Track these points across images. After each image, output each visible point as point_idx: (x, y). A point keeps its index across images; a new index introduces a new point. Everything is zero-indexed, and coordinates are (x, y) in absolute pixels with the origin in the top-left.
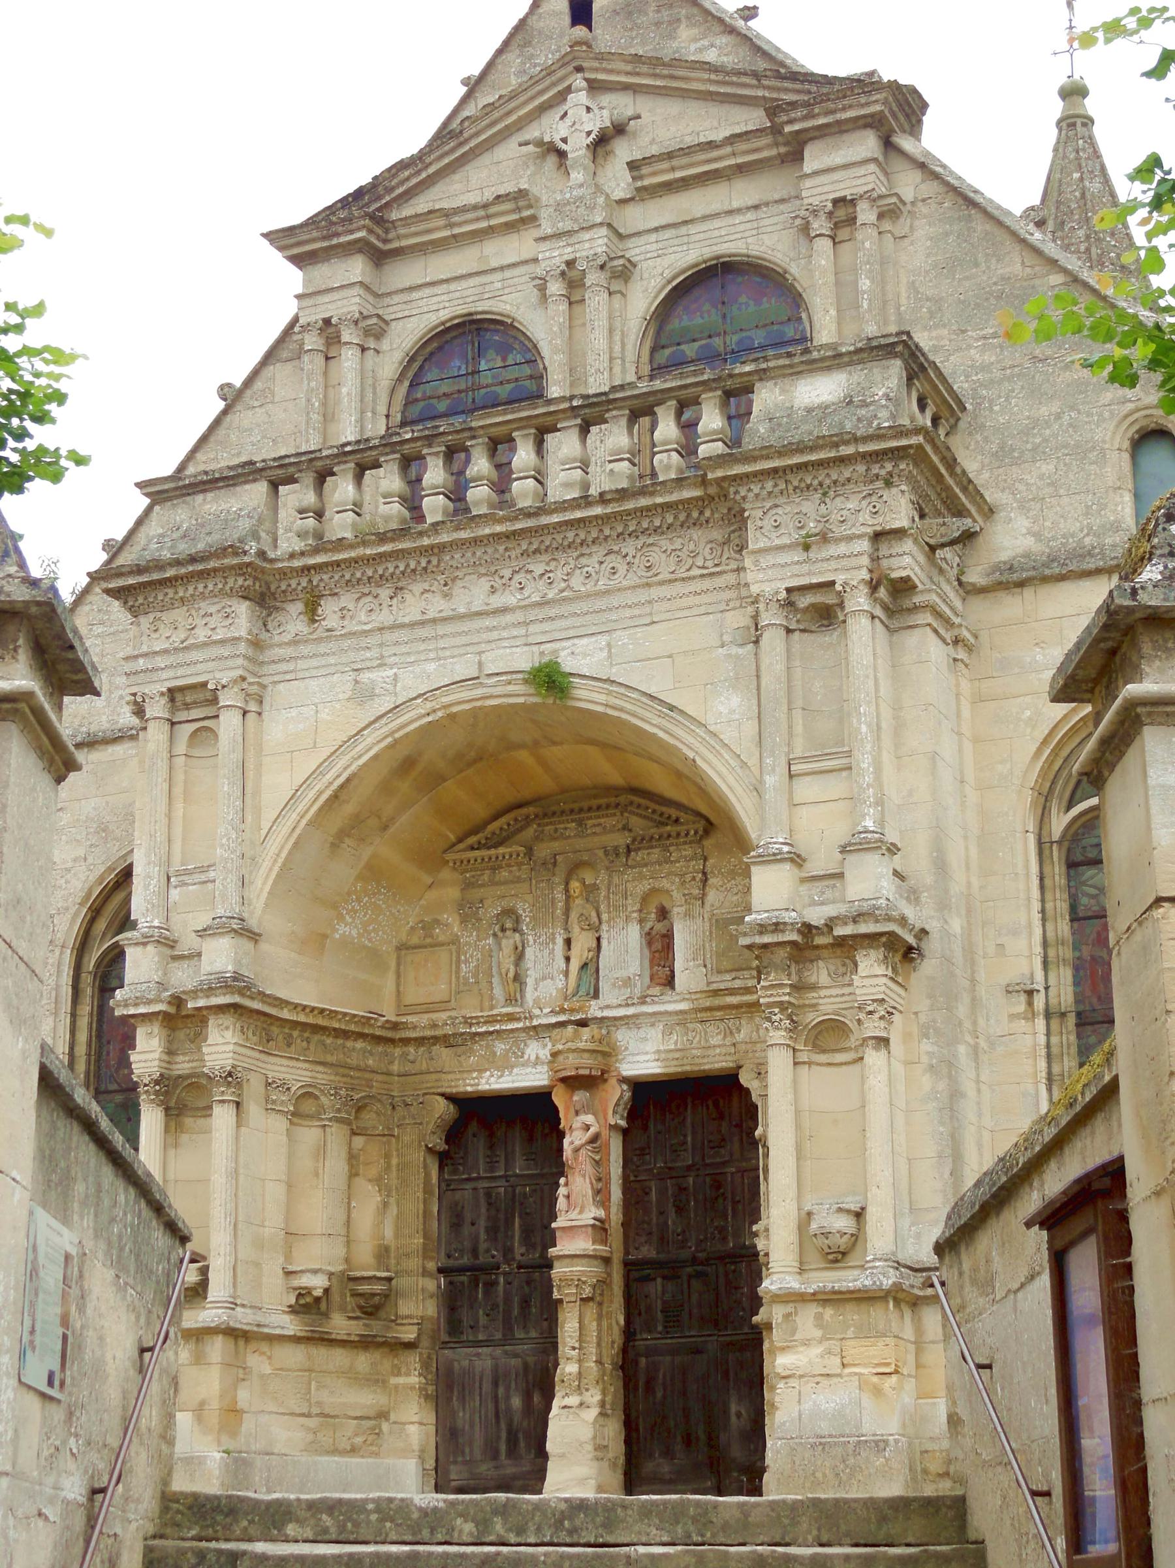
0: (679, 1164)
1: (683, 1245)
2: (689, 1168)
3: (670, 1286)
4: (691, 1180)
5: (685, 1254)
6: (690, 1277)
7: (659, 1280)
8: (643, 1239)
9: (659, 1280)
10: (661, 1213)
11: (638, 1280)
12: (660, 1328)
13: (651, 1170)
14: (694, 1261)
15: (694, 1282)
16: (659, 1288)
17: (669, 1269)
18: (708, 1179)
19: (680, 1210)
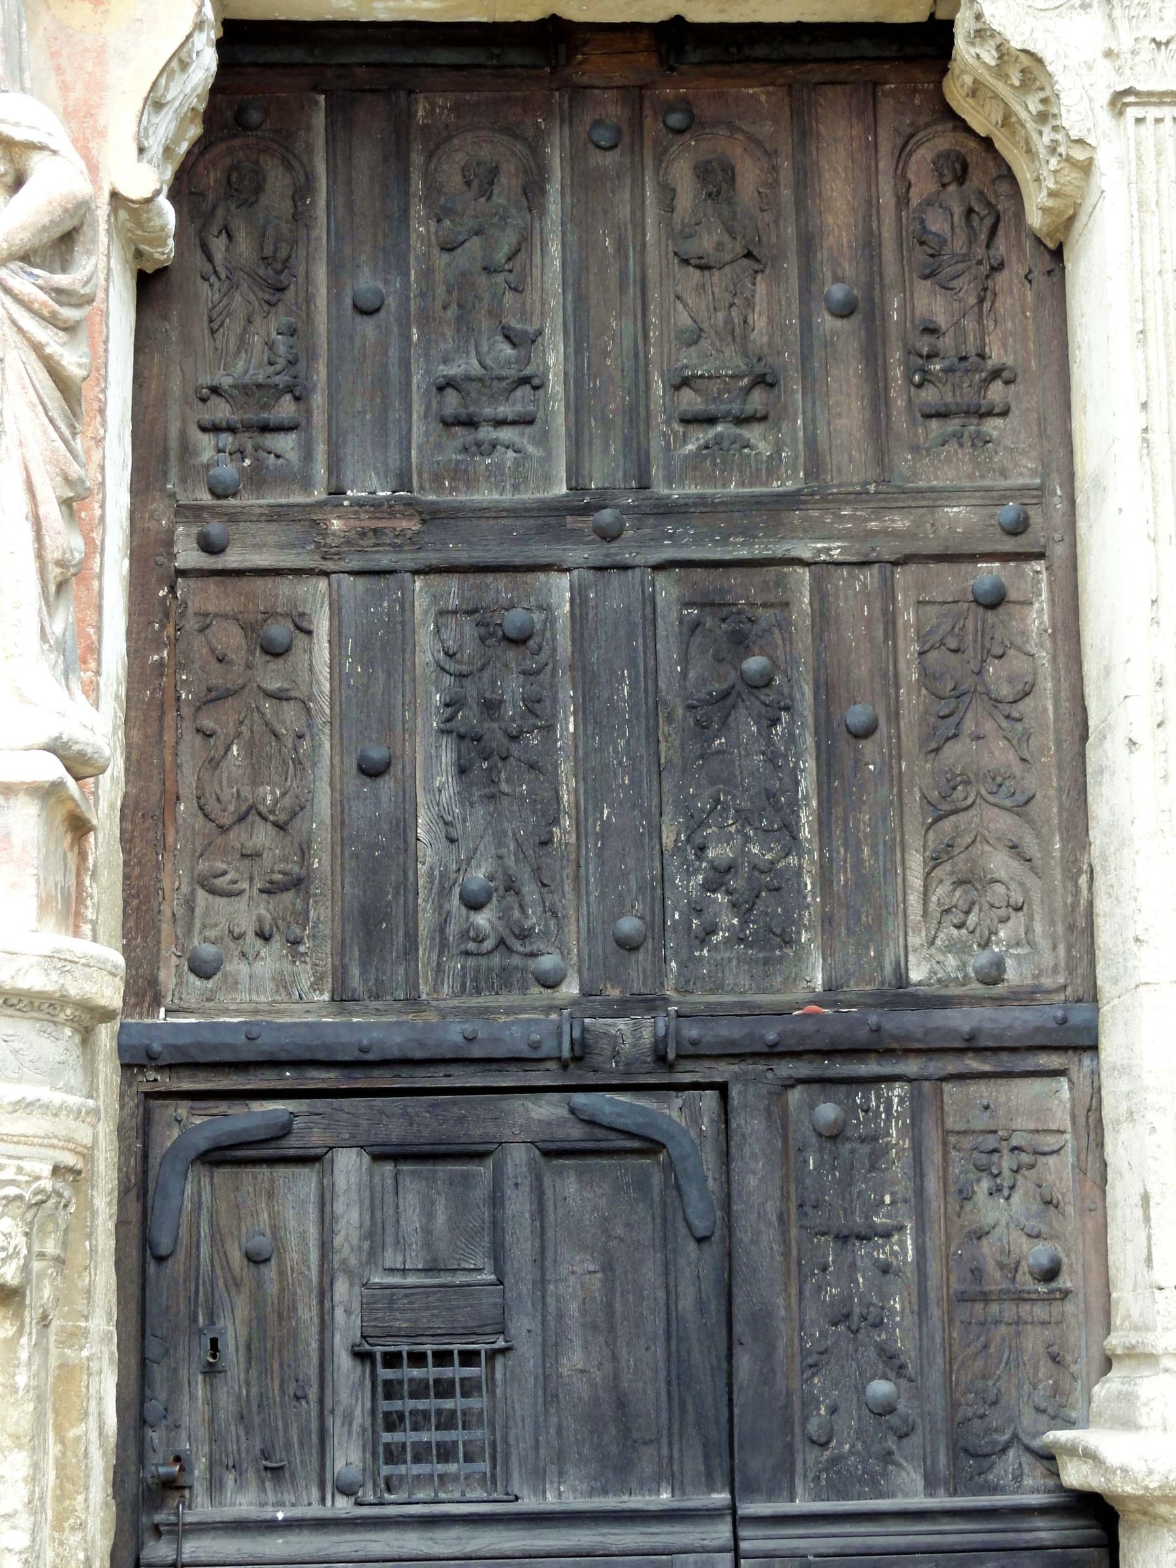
0: (485, 495)
1: (504, 961)
2: (553, 518)
3: (419, 1201)
4: (561, 587)
5: (523, 1020)
6: (555, 1153)
7: (349, 1165)
8: (245, 913)
9: (349, 1165)
10: (372, 771)
11: (220, 1156)
12: (347, 1457)
13: (307, 520)
14: (577, 1065)
15: (571, 1188)
16: (350, 1217)
17: (415, 1101)
18: (667, 590)
19: (487, 750)
